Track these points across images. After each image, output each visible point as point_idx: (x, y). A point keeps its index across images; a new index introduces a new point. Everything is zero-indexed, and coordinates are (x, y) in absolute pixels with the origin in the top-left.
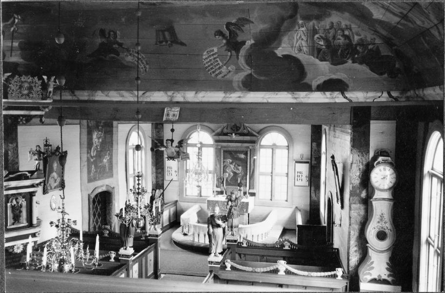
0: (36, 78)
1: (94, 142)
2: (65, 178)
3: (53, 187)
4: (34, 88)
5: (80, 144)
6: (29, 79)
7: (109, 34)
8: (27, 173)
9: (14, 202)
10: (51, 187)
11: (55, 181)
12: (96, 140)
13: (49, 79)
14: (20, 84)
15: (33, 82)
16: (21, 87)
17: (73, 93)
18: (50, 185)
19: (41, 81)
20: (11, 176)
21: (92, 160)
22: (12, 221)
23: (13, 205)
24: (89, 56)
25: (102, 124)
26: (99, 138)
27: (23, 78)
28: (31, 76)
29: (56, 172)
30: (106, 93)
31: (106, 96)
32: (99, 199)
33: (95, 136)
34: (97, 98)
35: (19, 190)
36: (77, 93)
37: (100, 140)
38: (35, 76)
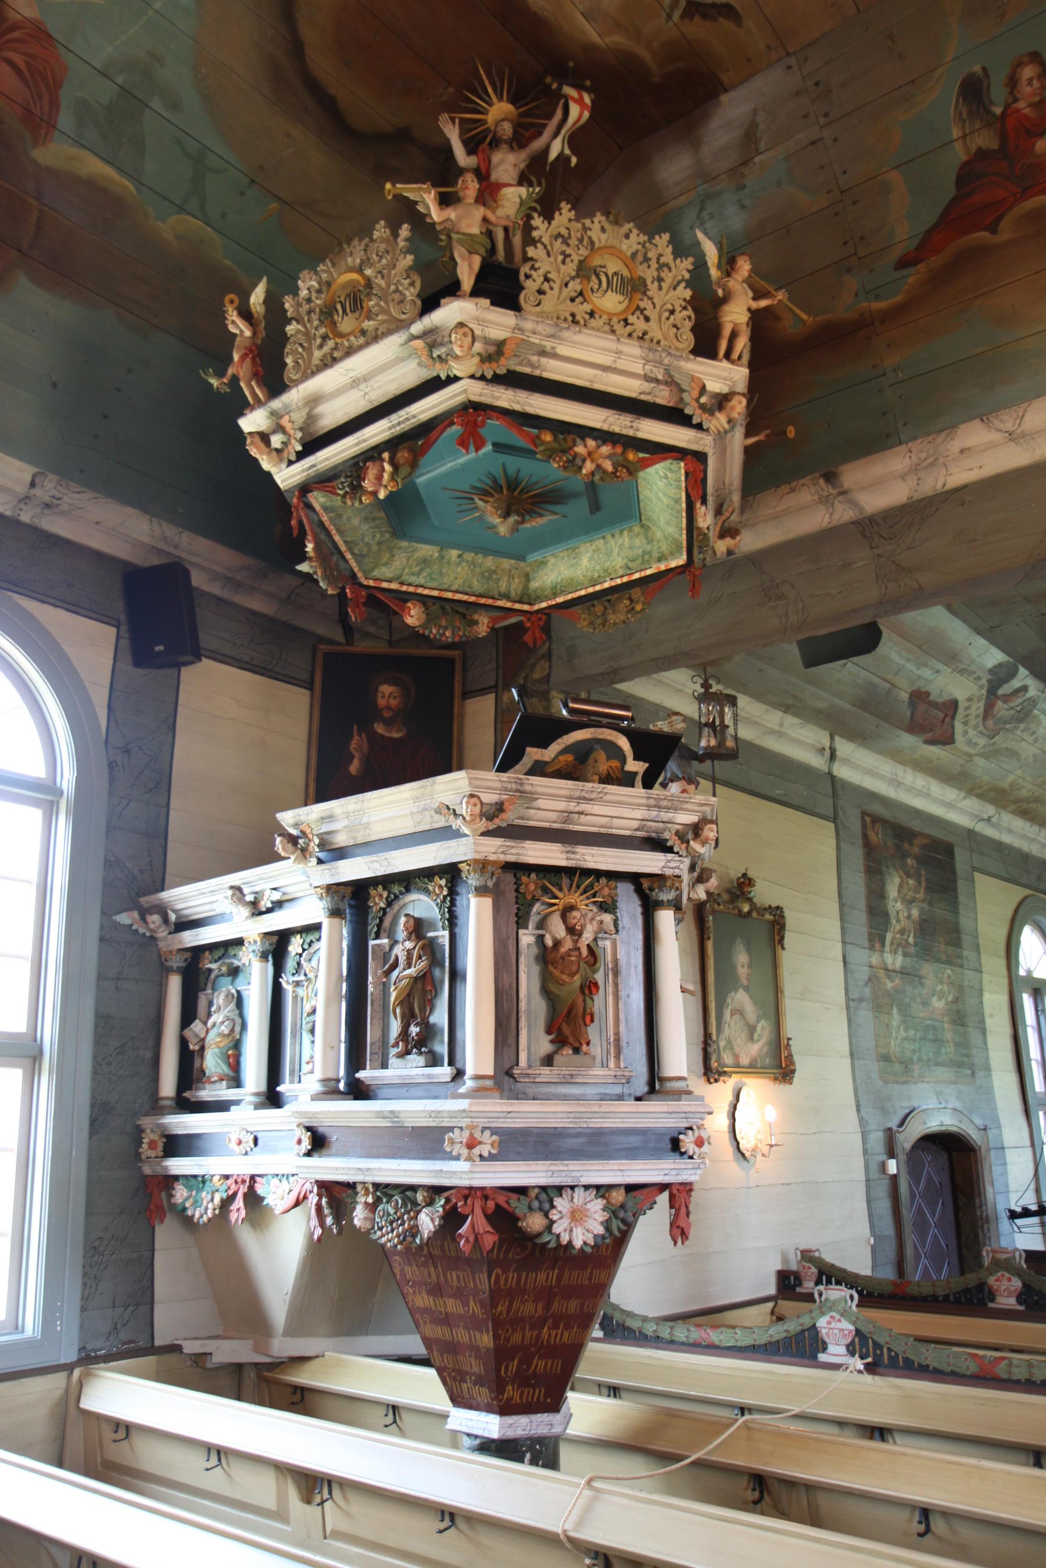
0: (663, 240)
1: (892, 913)
2: (791, 1027)
3: (745, 1061)
4: (653, 287)
5: (842, 905)
6: (627, 236)
7: (1013, 82)
8: (624, 743)
9: (557, 929)
10: (736, 1057)
11: (751, 1030)
12: (899, 905)
13: (728, 265)
14: (584, 252)
15: (646, 259)
16: (584, 271)
17: (830, 477)
18: (729, 1041)
19: (688, 263)
20: (533, 754)
21: (889, 985)
22: (545, 1045)
23: (549, 942)
24: (905, 263)
25: (916, 850)
26: (909, 902)
27: (596, 226)
28: (642, 229)
29: (747, 989)
30: (1007, 421)
31: (1012, 437)
32: (930, 1180)
33: (892, 891)
34: (960, 475)
35: (581, 849)
36: (852, 475)
37: (915, 913)
38: (659, 231)
